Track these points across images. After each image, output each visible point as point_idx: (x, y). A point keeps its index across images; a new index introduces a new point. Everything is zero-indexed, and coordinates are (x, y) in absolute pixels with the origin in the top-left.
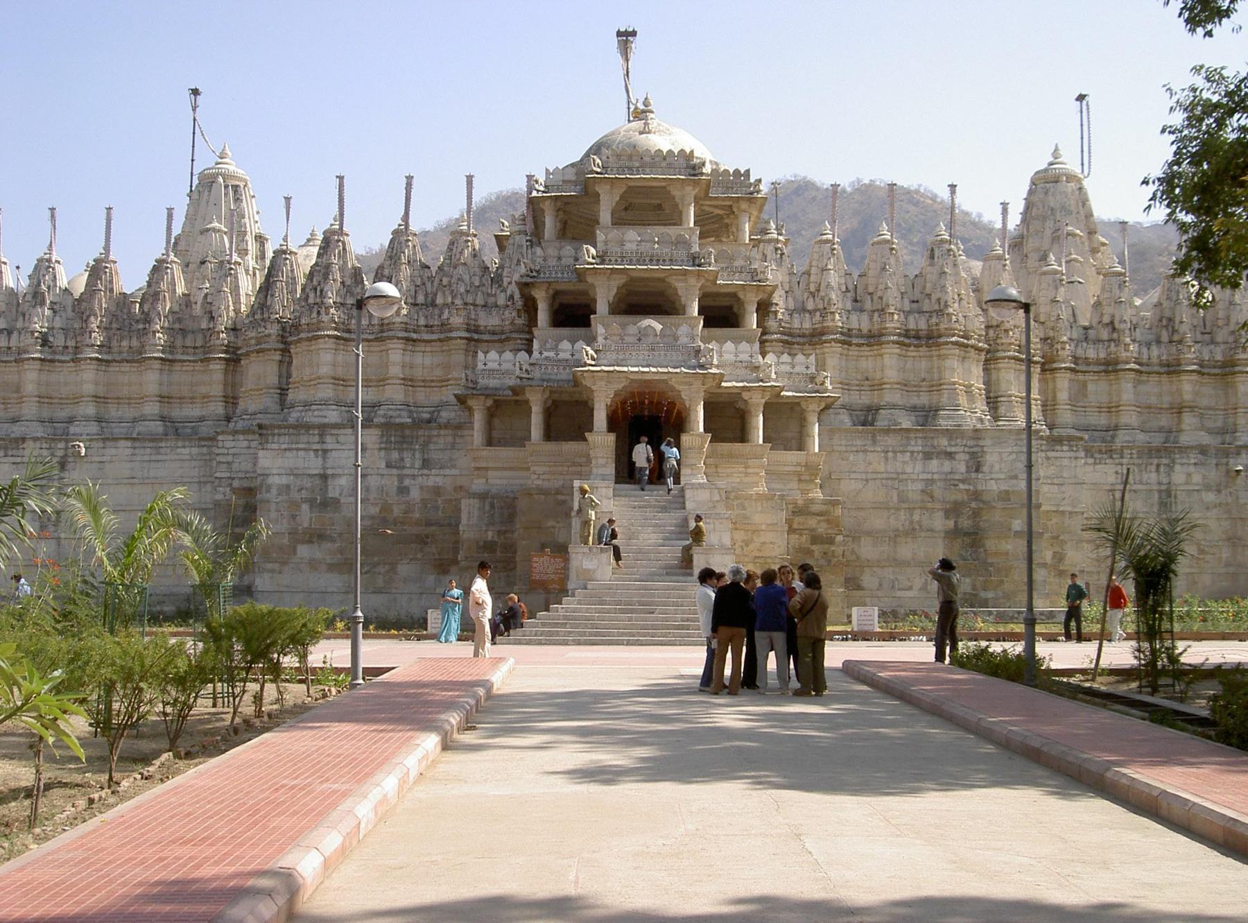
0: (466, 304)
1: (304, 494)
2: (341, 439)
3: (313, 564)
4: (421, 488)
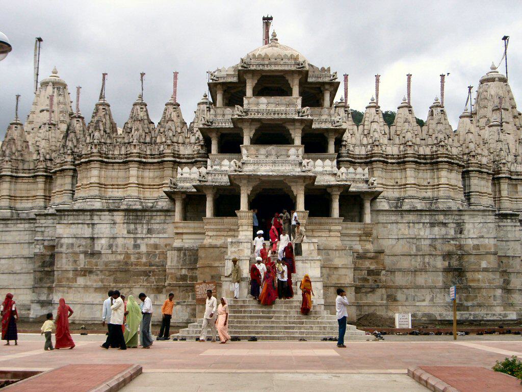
0: (173, 142)
1: (81, 249)
2: (103, 217)
3: (86, 288)
4: (147, 245)
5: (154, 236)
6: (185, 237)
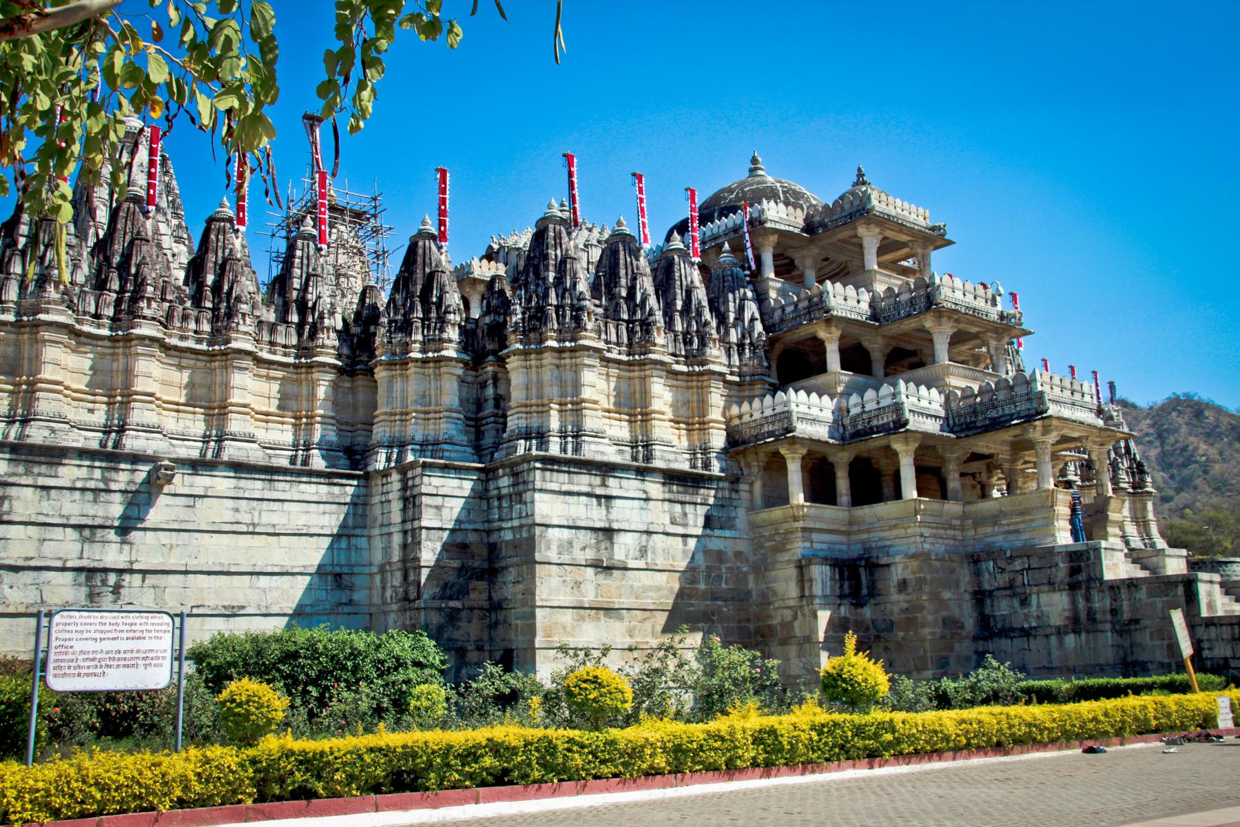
1: (590, 555)
2: (624, 482)
5: (717, 532)
6: (815, 536)
